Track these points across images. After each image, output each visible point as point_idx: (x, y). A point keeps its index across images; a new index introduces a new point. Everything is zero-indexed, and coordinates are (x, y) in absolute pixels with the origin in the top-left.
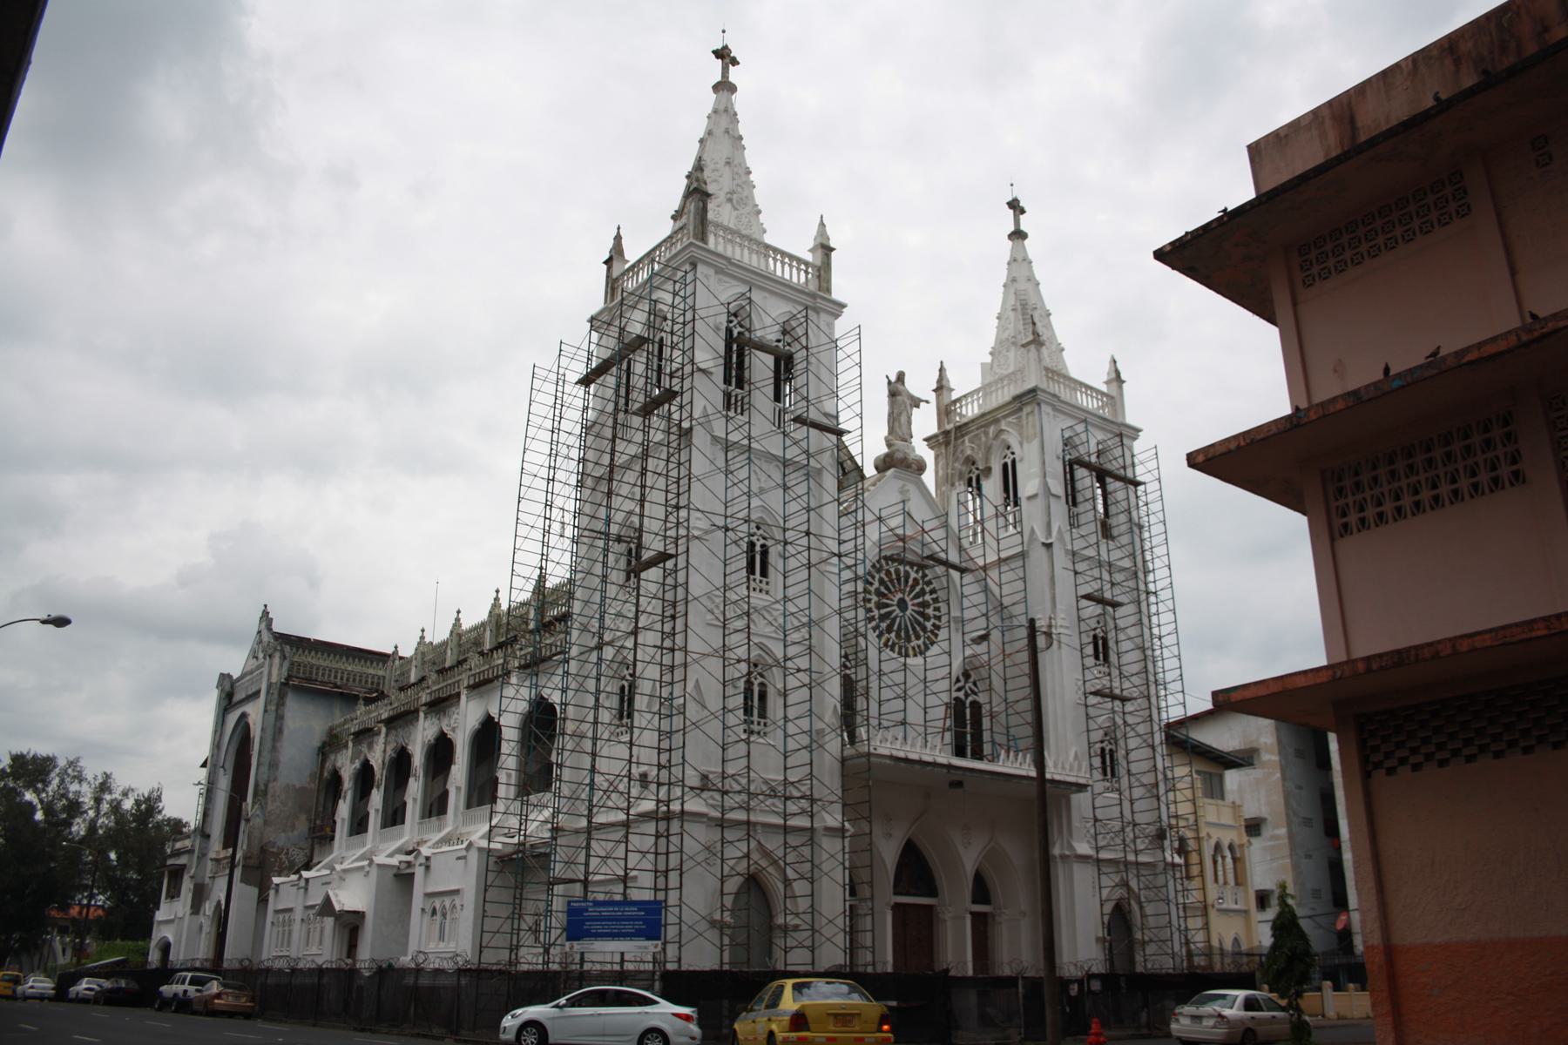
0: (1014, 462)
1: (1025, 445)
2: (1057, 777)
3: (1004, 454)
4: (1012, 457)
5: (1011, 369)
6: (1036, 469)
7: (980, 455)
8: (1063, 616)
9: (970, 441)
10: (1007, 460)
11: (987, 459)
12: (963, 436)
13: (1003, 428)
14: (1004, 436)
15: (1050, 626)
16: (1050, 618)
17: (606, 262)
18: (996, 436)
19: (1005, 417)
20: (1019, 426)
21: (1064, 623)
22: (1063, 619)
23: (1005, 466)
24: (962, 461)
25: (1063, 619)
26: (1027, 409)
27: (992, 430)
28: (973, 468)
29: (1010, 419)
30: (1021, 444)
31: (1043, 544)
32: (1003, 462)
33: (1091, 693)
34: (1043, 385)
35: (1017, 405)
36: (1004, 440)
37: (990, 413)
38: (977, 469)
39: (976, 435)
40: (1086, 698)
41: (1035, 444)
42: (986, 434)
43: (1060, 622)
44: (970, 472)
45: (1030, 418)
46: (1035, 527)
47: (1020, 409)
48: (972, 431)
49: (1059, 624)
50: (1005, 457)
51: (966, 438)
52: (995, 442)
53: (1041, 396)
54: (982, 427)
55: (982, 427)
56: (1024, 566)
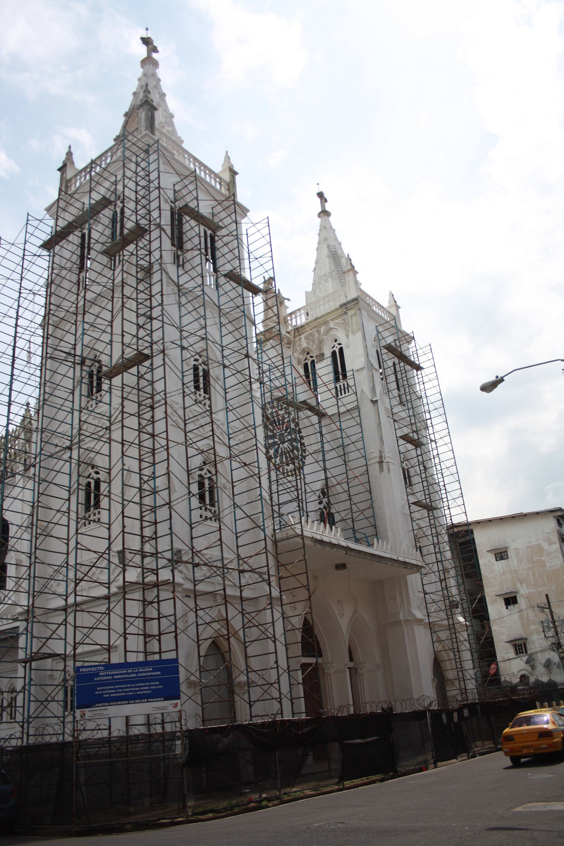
0: (341, 350)
1: (351, 336)
2: (407, 560)
3: (332, 345)
4: (339, 347)
5: (331, 291)
6: (361, 351)
7: (315, 347)
8: (388, 450)
9: (306, 338)
10: (335, 349)
11: (320, 349)
12: (300, 335)
13: (332, 327)
14: (331, 333)
15: (381, 457)
16: (380, 452)
17: (59, 170)
18: (327, 332)
19: (333, 319)
20: (345, 325)
21: (391, 455)
22: (388, 452)
23: (334, 353)
24: (300, 352)
25: (388, 452)
26: (351, 313)
27: (323, 329)
28: (308, 356)
29: (337, 321)
30: (347, 336)
31: (371, 400)
32: (332, 350)
33: (413, 503)
34: (362, 297)
35: (340, 311)
36: (332, 335)
37: (320, 317)
38: (311, 357)
39: (311, 334)
40: (410, 507)
41: (359, 335)
42: (319, 332)
43: (387, 455)
44: (306, 359)
45: (354, 318)
46: (364, 390)
47: (346, 313)
48: (307, 331)
49: (387, 456)
50: (333, 347)
51: (302, 336)
52: (325, 337)
53: (361, 303)
54: (315, 327)
55: (315, 327)
56: (359, 416)
